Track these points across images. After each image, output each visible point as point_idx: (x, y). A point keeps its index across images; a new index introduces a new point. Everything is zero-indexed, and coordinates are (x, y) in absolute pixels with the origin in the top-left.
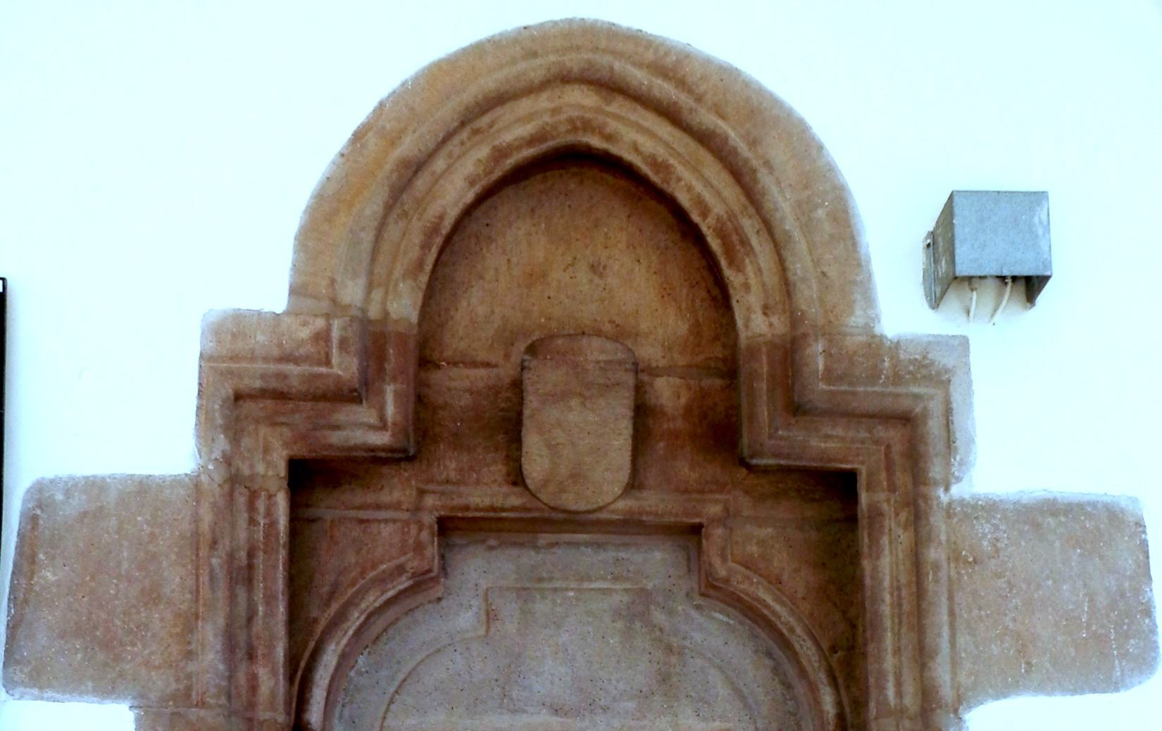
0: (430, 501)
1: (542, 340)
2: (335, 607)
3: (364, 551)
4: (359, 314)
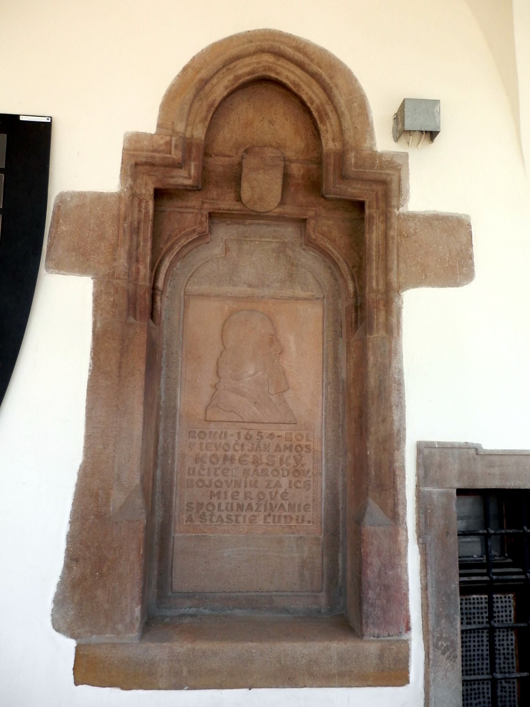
0: (206, 206)
1: (250, 148)
2: (169, 244)
3: (181, 223)
4: (182, 135)
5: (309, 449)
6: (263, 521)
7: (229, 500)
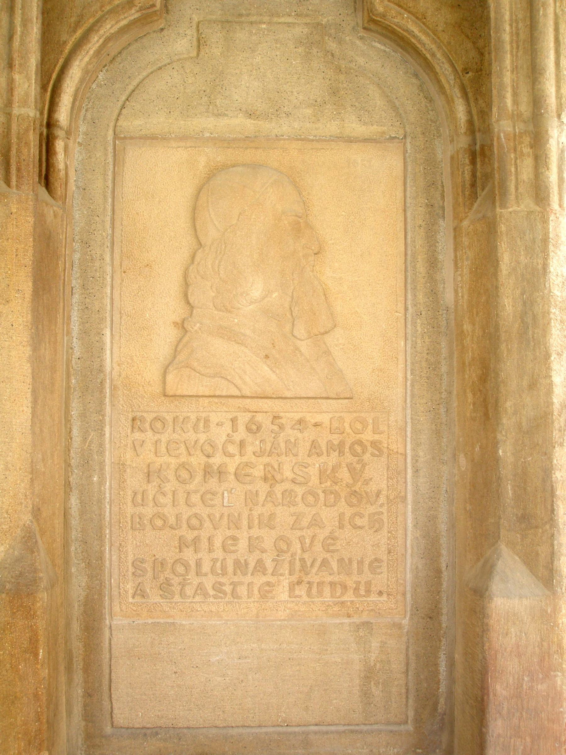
5: (379, 450)
6: (287, 593)
7: (219, 554)
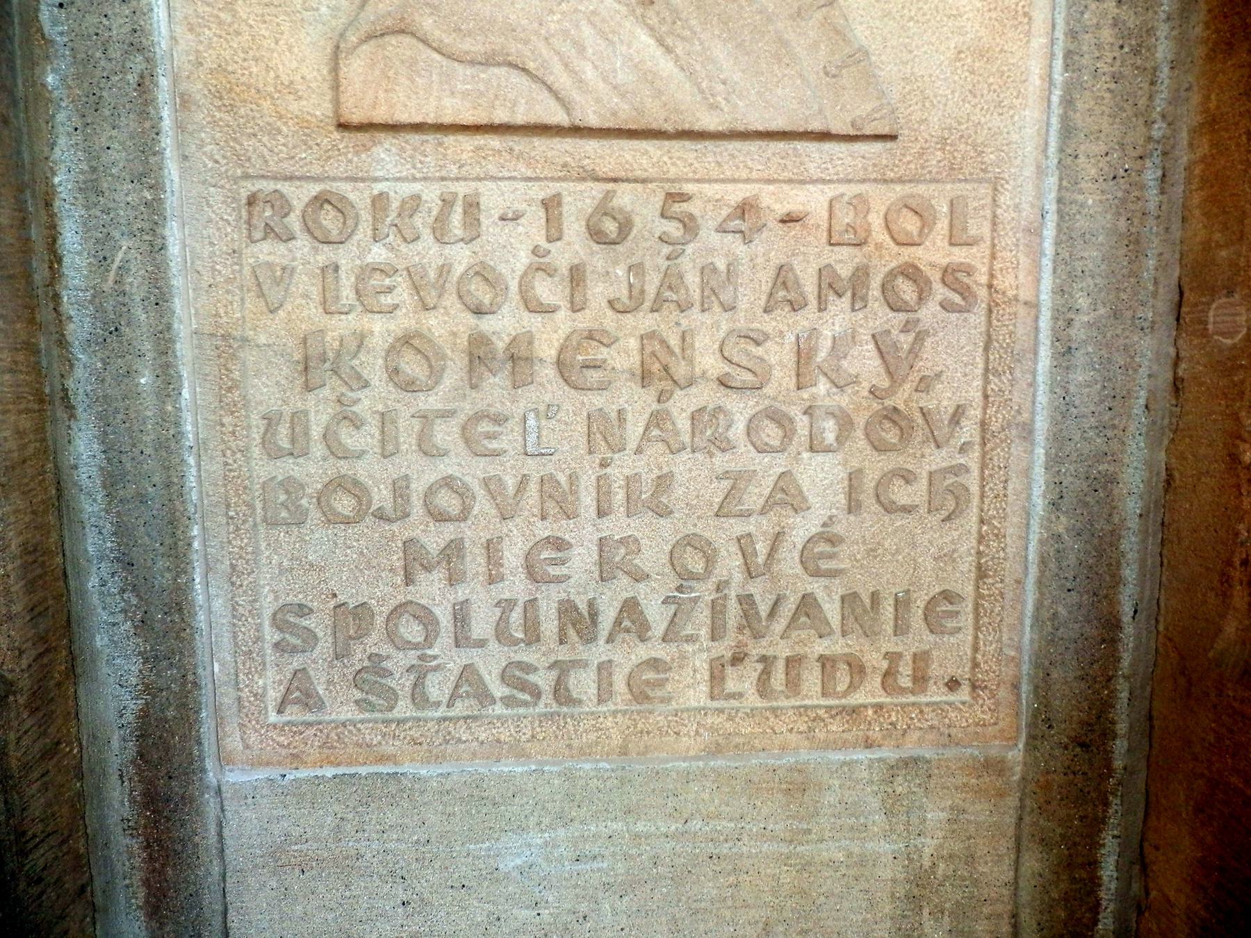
5: (965, 292)
6: (704, 688)
7: (516, 586)
